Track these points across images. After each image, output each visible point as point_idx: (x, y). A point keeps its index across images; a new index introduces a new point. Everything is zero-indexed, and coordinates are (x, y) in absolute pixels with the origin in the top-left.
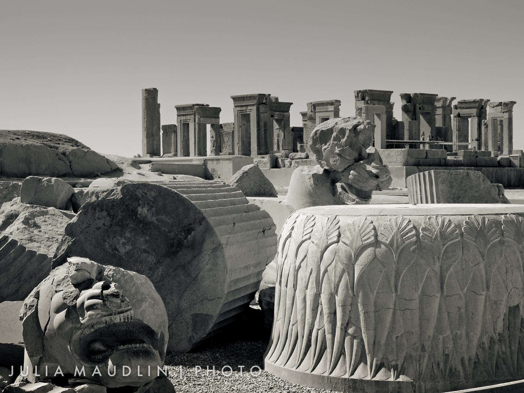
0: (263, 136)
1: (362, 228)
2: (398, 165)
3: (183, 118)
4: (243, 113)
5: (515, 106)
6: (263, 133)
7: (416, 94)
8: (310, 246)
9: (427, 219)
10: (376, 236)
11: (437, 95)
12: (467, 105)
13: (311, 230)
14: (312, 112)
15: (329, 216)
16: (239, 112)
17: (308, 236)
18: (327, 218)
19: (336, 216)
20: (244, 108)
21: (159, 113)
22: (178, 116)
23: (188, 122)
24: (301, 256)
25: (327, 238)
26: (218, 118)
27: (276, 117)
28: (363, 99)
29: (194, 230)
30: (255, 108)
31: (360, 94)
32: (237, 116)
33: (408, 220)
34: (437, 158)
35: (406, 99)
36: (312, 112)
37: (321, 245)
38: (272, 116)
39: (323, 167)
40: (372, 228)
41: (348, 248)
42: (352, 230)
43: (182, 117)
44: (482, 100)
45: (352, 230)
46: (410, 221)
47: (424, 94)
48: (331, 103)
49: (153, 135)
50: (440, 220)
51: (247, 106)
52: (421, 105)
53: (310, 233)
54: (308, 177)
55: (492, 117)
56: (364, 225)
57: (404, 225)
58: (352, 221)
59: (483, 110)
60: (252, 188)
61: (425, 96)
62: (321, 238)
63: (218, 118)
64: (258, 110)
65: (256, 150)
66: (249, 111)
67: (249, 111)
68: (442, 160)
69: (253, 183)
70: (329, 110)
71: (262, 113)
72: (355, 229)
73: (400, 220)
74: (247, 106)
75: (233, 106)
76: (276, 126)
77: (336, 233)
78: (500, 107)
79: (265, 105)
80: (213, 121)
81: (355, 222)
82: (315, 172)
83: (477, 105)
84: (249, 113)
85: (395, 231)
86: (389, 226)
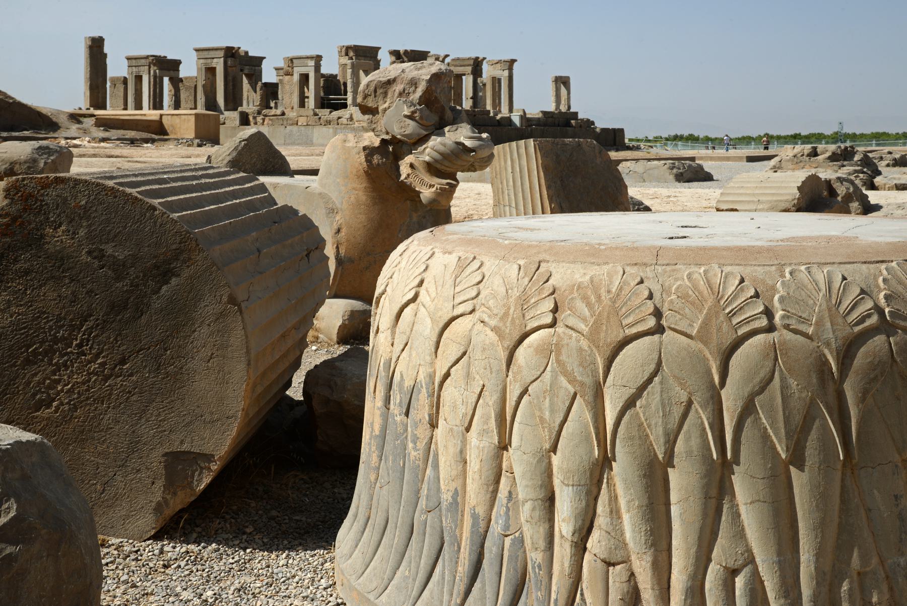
1: (618, 295)
3: (134, 69)
5: (515, 64)
7: (406, 51)
8: (475, 332)
9: (788, 275)
10: (658, 314)
11: (429, 52)
12: (462, 63)
13: (474, 294)
14: (289, 66)
15: (522, 262)
17: (467, 307)
18: (516, 267)
19: (540, 262)
20: (209, 61)
22: (129, 66)
24: (449, 351)
25: (524, 315)
26: (178, 70)
27: (246, 71)
28: (347, 54)
29: (179, 275)
30: (222, 59)
32: (199, 70)
33: (739, 278)
35: (395, 56)
36: (289, 66)
37: (508, 331)
38: (242, 70)
39: (378, 136)
40: (646, 297)
41: (584, 344)
42: (593, 299)
43: (134, 68)
44: (477, 58)
45: (593, 299)
46: (742, 281)
48: (311, 58)
50: (820, 277)
53: (473, 299)
54: (356, 150)
56: (621, 287)
57: (731, 289)
58: (588, 278)
59: (479, 68)
60: (255, 163)
62: (506, 314)
64: (225, 63)
69: (256, 156)
71: (230, 67)
72: (599, 297)
73: (715, 275)
74: (213, 58)
75: (196, 58)
76: (245, 81)
77: (549, 305)
78: (499, 65)
79: (233, 59)
80: (172, 73)
81: (595, 279)
82: (366, 143)
83: (472, 62)
85: (709, 304)
86: (690, 292)
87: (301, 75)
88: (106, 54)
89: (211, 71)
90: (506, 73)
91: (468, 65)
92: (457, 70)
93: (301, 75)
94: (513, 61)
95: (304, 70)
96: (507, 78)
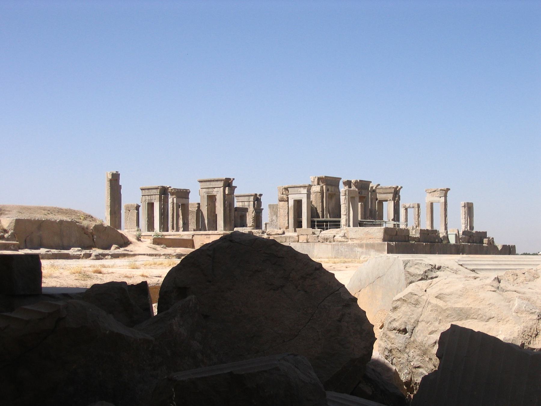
0: (228, 214)
2: (377, 241)
4: (209, 194)
5: (449, 192)
6: (228, 212)
16: (205, 193)
21: (120, 193)
22: (143, 196)
23: (153, 202)
26: (188, 198)
31: (316, 179)
32: (202, 197)
34: (403, 235)
43: (147, 197)
47: (362, 181)
49: (115, 213)
51: (214, 188)
52: (360, 190)
55: (430, 201)
61: (363, 182)
63: (187, 198)
65: (223, 227)
66: (216, 192)
67: (216, 192)
68: (406, 237)
70: (302, 193)
74: (214, 188)
79: (230, 188)
83: (393, 191)
84: (216, 194)
87: (295, 201)
88: (121, 186)
89: (212, 199)
90: (443, 200)
91: (390, 193)
92: (381, 197)
93: (295, 201)
94: (448, 189)
95: (298, 197)
96: (444, 203)
